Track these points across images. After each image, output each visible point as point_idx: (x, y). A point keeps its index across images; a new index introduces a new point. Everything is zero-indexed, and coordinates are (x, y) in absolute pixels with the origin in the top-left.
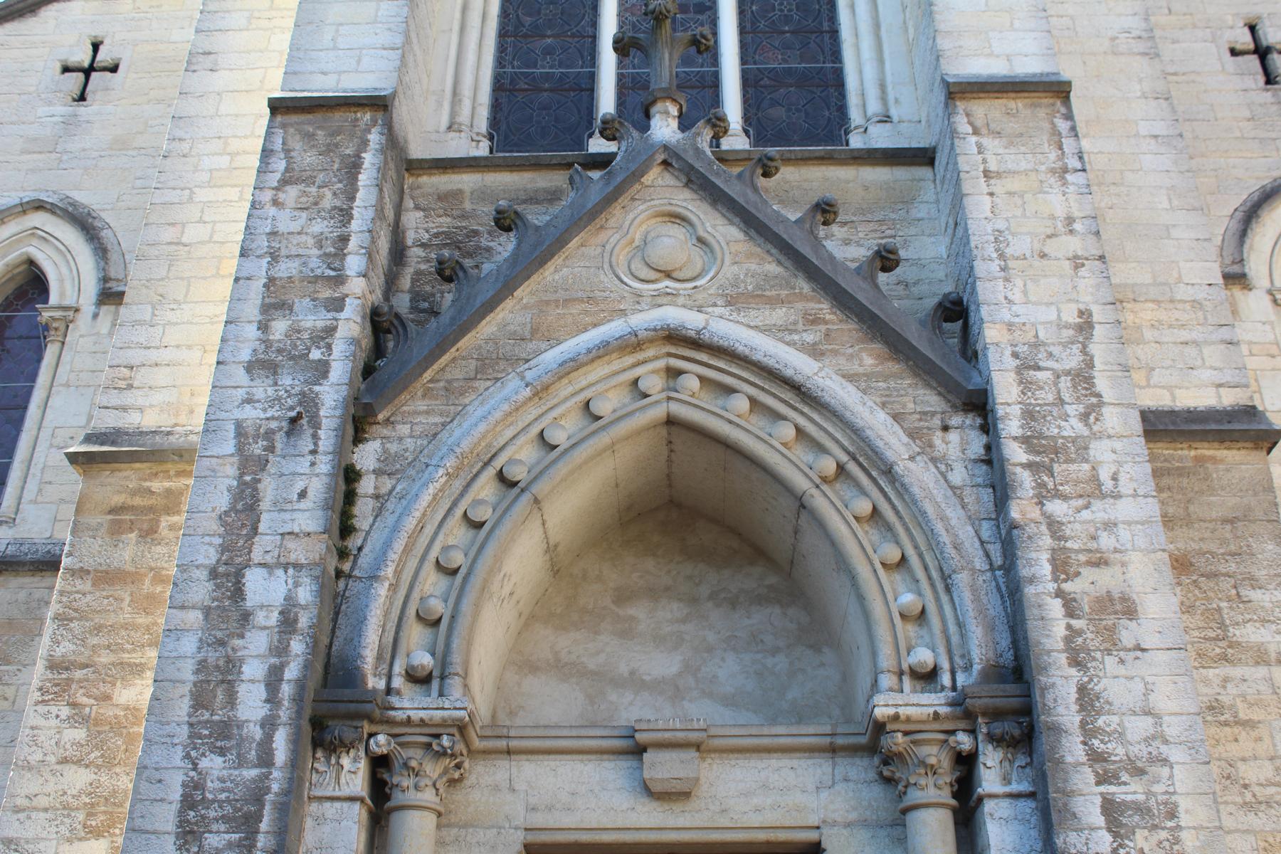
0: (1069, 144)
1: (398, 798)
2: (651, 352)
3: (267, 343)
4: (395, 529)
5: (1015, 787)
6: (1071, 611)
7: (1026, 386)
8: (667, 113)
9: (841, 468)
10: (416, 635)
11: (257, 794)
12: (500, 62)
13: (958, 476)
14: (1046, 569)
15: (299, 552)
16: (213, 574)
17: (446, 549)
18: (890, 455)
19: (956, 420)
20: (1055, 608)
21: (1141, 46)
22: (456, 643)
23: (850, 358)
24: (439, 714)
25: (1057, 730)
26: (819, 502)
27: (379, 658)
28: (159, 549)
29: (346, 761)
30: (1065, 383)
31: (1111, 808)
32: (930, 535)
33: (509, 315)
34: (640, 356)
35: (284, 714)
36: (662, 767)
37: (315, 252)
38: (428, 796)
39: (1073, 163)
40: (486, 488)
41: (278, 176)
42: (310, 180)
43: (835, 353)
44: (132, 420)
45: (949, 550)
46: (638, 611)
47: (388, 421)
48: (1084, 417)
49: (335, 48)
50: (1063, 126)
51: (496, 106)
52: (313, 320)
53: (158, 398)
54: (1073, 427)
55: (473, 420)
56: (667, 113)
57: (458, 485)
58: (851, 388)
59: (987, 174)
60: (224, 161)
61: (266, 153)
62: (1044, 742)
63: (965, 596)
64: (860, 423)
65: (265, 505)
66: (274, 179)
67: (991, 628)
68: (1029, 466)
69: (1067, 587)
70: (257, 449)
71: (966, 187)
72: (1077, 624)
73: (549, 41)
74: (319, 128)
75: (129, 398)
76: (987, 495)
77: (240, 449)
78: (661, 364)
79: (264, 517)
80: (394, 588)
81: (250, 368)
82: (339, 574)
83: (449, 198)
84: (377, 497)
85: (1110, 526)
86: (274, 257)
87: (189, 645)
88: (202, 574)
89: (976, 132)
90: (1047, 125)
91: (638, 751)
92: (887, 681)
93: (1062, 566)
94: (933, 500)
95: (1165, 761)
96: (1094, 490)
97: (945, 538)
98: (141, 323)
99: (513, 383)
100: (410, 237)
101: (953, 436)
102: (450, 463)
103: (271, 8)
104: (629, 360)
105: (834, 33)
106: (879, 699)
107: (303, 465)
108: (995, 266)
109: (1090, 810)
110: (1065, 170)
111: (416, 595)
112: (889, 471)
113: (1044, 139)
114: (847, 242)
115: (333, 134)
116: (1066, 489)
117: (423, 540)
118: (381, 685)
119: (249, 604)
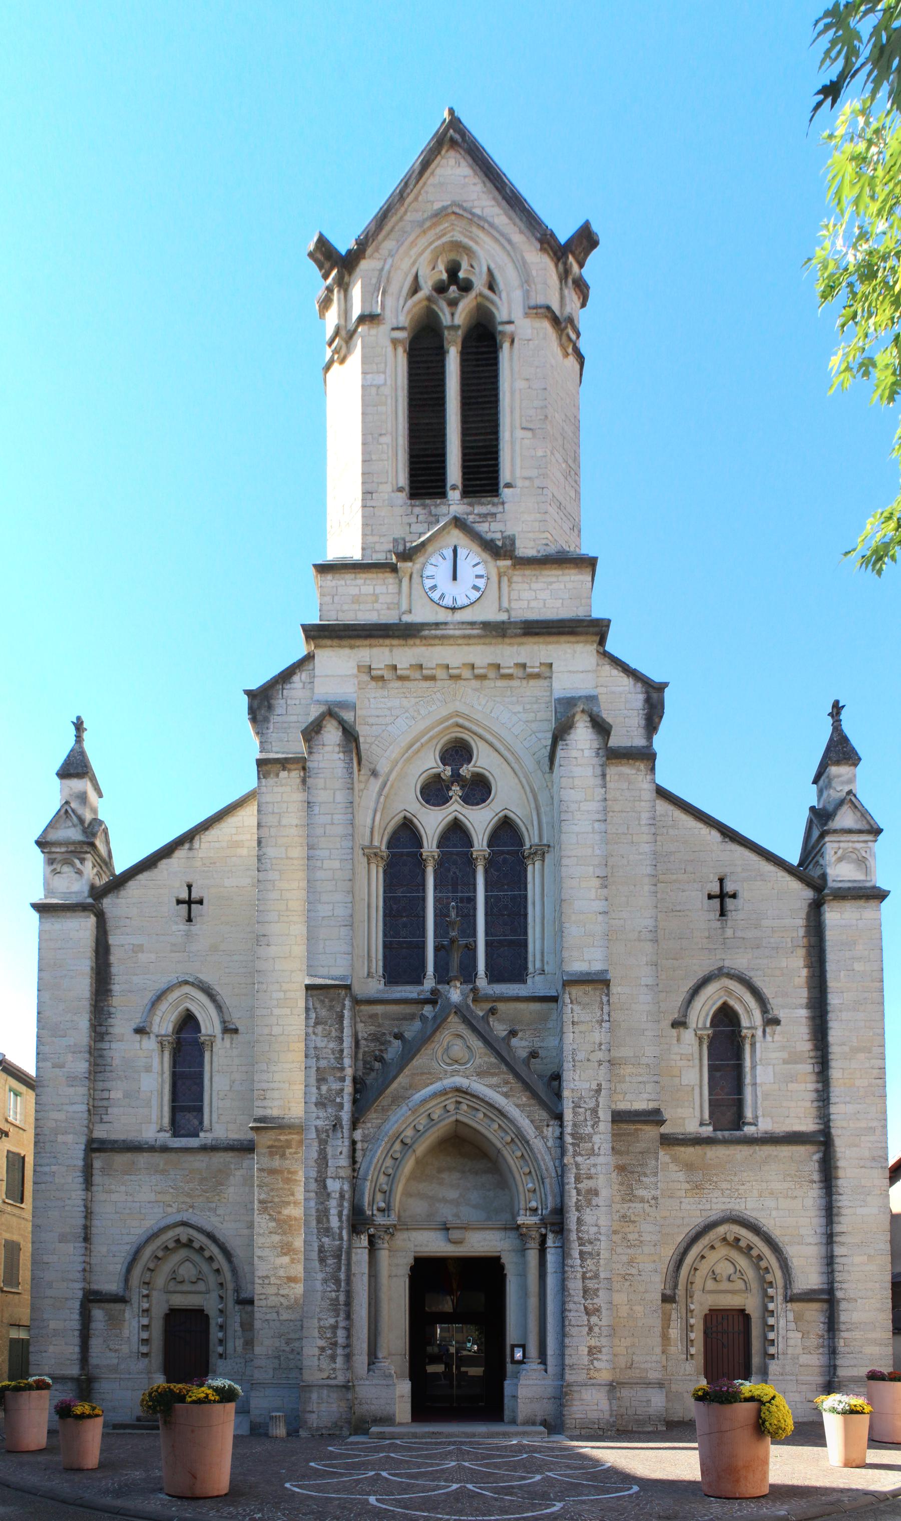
0: (606, 1008)
1: (377, 1246)
2: (450, 1095)
3: (321, 1095)
4: (370, 1162)
5: (556, 1245)
6: (578, 1194)
7: (575, 1114)
8: (456, 987)
9: (512, 1140)
10: (379, 1196)
11: (340, 1248)
12: (385, 935)
13: (550, 1144)
14: (573, 1180)
15: (342, 1173)
16: (316, 1180)
17: (386, 1168)
18: (528, 1137)
19: (551, 1123)
20: (574, 1192)
21: (650, 936)
22: (392, 1200)
23: (518, 1098)
24: (389, 1223)
25: (569, 1231)
26: (505, 1153)
27: (369, 1204)
28: (287, 1162)
29: (362, 1237)
30: (588, 1113)
31: (581, 1253)
32: (539, 1165)
33: (402, 1080)
34: (447, 1097)
35: (345, 1224)
36: (455, 1235)
37: (332, 1056)
38: (386, 1245)
39: (606, 1017)
40: (397, 1146)
41: (313, 1020)
42: (325, 1023)
43: (513, 1096)
44: (268, 1112)
45: (545, 1171)
46: (445, 1175)
47: (363, 1122)
48: (593, 1126)
49: (325, 953)
50: (605, 999)
51: (385, 957)
52: (336, 1086)
53: (276, 1103)
54: (589, 1130)
55: (391, 1123)
56: (456, 987)
57: (389, 1145)
58: (517, 1110)
59: (573, 1023)
60: (281, 995)
61: (307, 1009)
62: (565, 1233)
63: (548, 1186)
64: (519, 1125)
65: (329, 1156)
66: (312, 1022)
67: (554, 1196)
68: (572, 1144)
69: (579, 1186)
70: (324, 1136)
71: (565, 1030)
72: (580, 1198)
73: (405, 919)
74: (326, 997)
75: (266, 1103)
76: (559, 1150)
77: (318, 1136)
78: (454, 1100)
79: (330, 1161)
80: (372, 1182)
81: (316, 1105)
82: (354, 1177)
83: (373, 1016)
84: (363, 1150)
85: (595, 1165)
86: (318, 1059)
87: (312, 1204)
88: (313, 1181)
89: (572, 1003)
90: (599, 999)
91: (448, 1229)
92: (522, 1212)
93: (578, 1179)
94: (540, 1153)
95: (599, 1240)
96: (592, 1153)
97: (543, 1167)
98: (262, 1071)
99: (405, 1108)
100: (360, 1035)
101: (550, 1129)
102: (386, 1139)
103: (287, 910)
104: (443, 1098)
105: (526, 915)
106: (519, 1218)
107: (339, 1142)
108: (571, 1065)
109: (576, 1254)
110: (602, 1021)
111: (378, 1184)
112: (527, 1142)
113: (596, 1007)
114: (521, 1039)
115: (331, 1000)
116: (583, 1152)
117: (379, 1165)
118: (370, 1213)
119: (329, 1190)
